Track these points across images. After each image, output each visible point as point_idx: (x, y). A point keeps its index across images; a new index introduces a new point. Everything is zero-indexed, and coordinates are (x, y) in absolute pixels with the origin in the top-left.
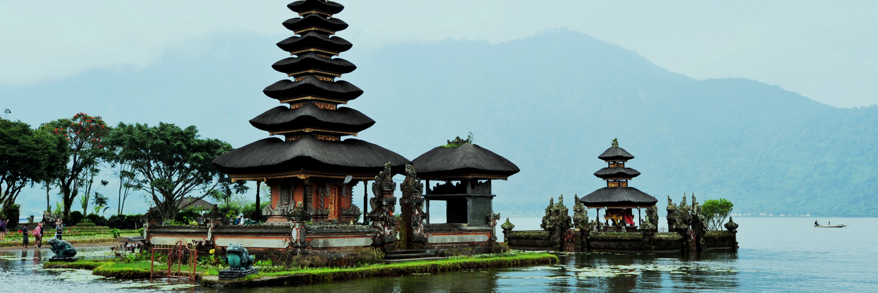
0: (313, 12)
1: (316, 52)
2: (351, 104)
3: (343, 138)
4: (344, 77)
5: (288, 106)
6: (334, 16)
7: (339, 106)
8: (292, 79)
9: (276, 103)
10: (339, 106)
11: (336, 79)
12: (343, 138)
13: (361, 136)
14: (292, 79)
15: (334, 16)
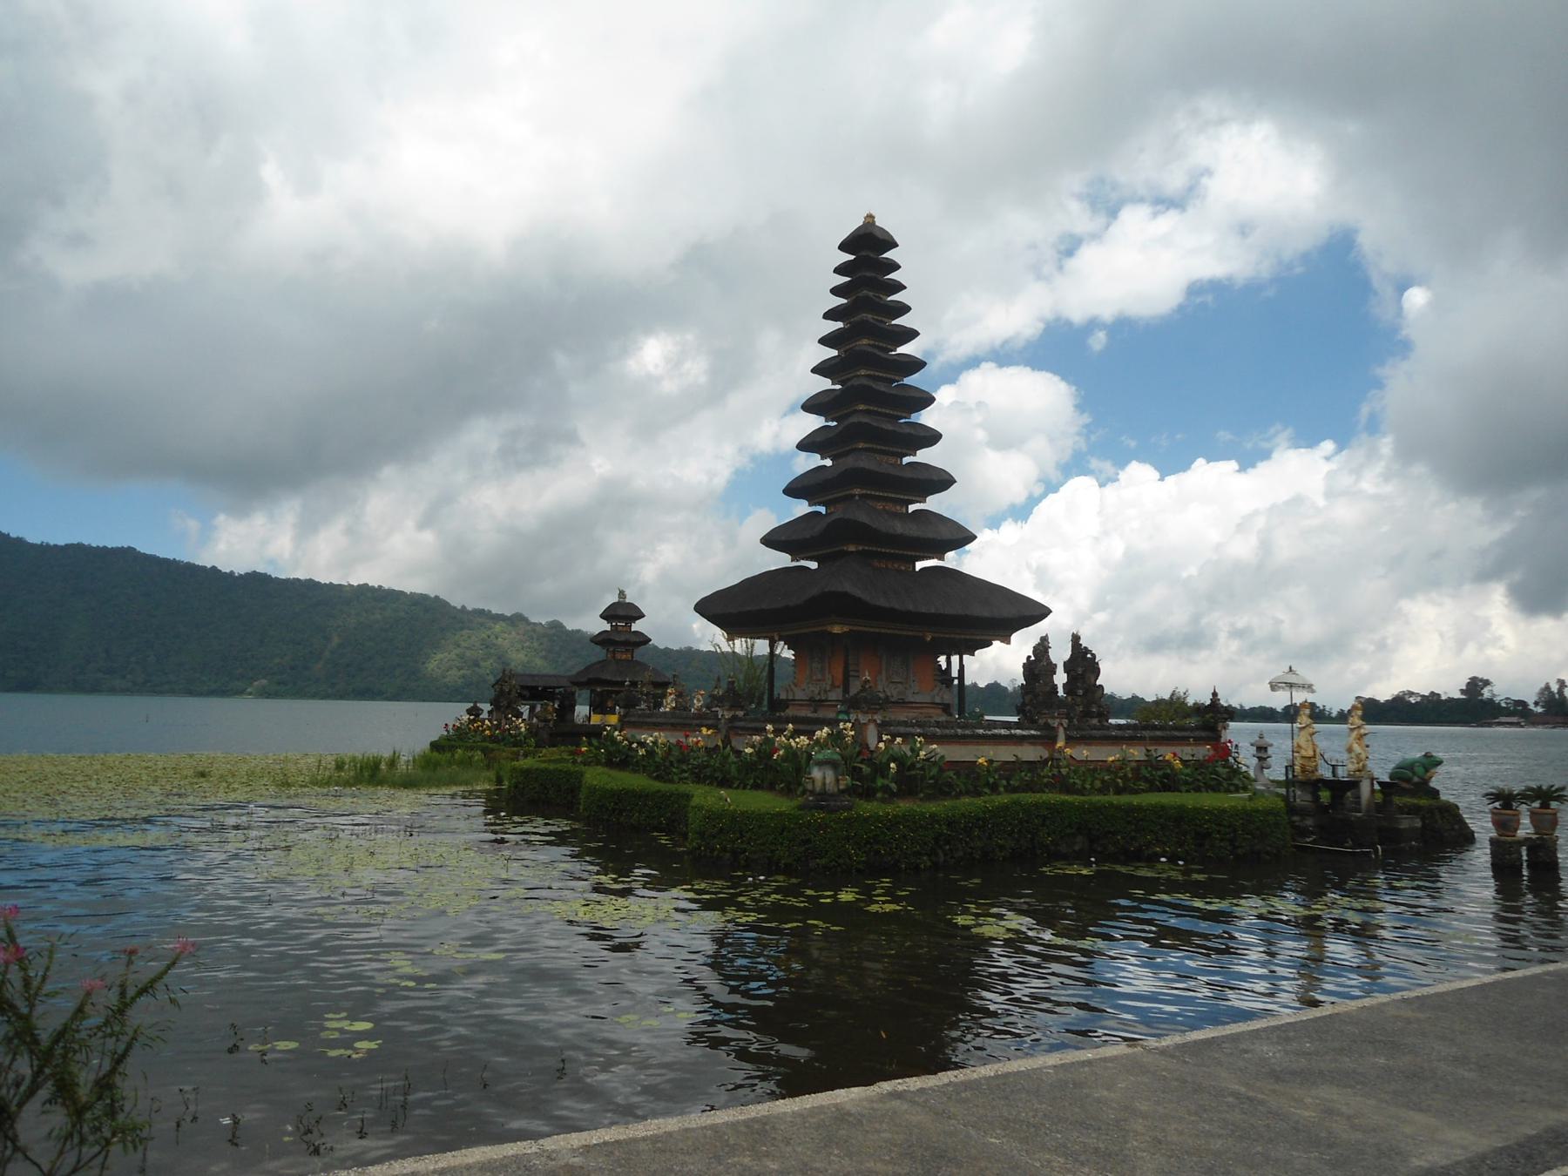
0: (865, 341)
1: (868, 412)
2: (934, 503)
3: (919, 565)
4: (924, 456)
5: (822, 509)
6: (901, 350)
7: (912, 508)
8: (828, 462)
9: (801, 508)
10: (912, 508)
11: (906, 460)
12: (919, 565)
13: (951, 560)
14: (828, 462)
15: (901, 350)
